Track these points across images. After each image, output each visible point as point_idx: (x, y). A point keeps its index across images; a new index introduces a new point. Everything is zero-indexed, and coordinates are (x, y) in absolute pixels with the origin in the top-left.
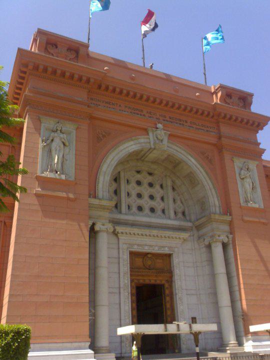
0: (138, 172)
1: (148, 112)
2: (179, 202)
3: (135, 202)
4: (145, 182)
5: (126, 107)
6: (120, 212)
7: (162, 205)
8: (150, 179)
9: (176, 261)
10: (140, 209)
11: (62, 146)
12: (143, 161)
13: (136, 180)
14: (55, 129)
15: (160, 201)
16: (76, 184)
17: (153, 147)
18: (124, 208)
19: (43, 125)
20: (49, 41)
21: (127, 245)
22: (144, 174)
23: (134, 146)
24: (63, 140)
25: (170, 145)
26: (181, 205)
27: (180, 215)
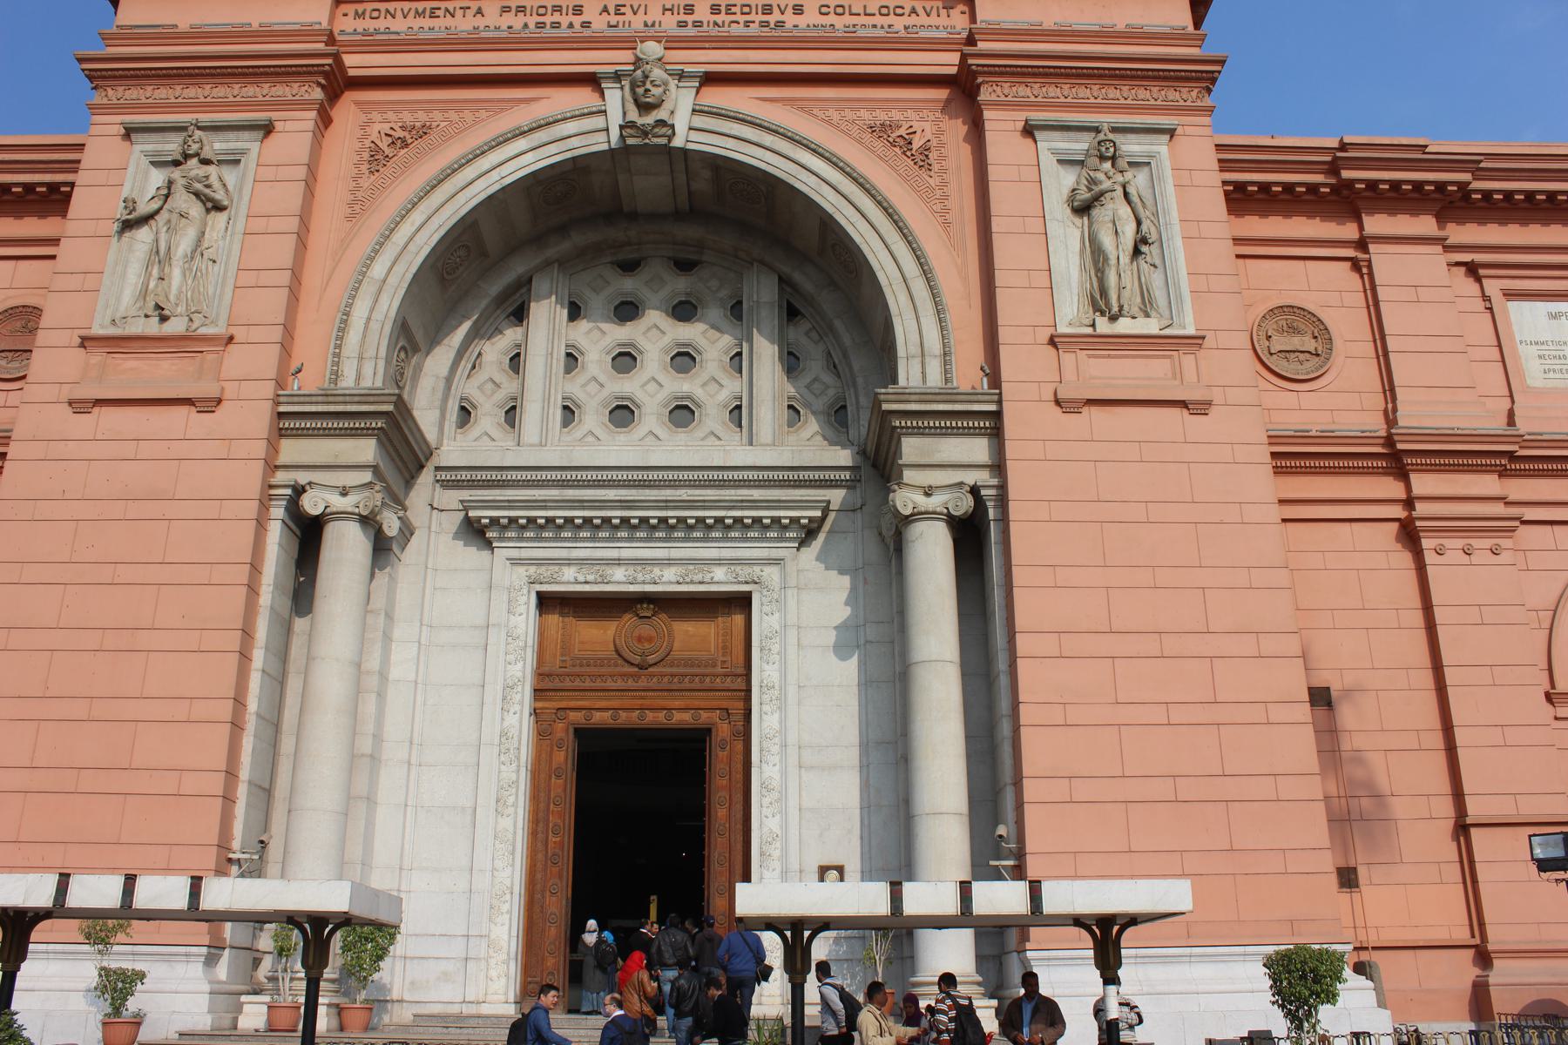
0: (629, 267)
2: (815, 367)
3: (597, 384)
7: (732, 386)
8: (680, 285)
9: (764, 620)
11: (195, 209)
12: (633, 216)
19: (138, 148)
21: (532, 569)
23: (529, 157)
24: (199, 186)
25: (700, 121)
26: (828, 378)
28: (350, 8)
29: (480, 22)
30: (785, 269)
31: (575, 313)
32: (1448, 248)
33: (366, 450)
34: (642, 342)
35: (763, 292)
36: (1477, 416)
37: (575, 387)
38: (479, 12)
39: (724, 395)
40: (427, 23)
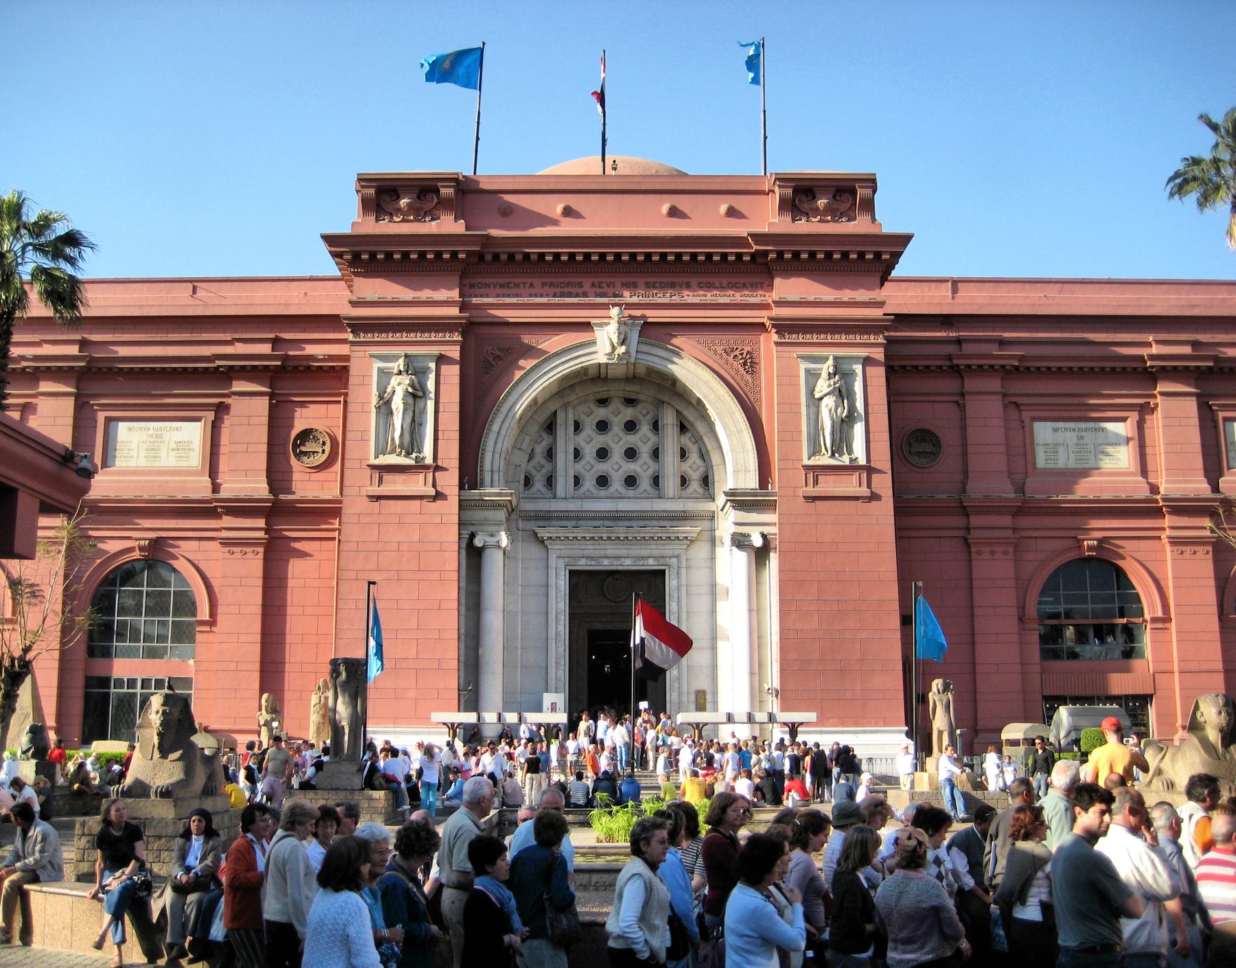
0: (603, 402)
1: (593, 285)
2: (694, 457)
3: (591, 468)
4: (617, 423)
5: (544, 284)
6: (555, 497)
7: (652, 467)
8: (629, 413)
9: (671, 583)
10: (603, 481)
11: (411, 400)
13: (597, 420)
14: (396, 371)
15: (650, 462)
16: (437, 468)
17: (602, 359)
18: (563, 484)
20: (382, 194)
22: (616, 404)
24: (410, 390)
25: (644, 348)
26: (699, 462)
27: (695, 486)
28: (467, 282)
29: (532, 291)
30: (681, 409)
31: (577, 427)
32: (1004, 395)
33: (501, 515)
34: (611, 443)
35: (669, 419)
36: (1004, 490)
37: (579, 467)
38: (531, 285)
39: (650, 472)
40: (506, 291)
